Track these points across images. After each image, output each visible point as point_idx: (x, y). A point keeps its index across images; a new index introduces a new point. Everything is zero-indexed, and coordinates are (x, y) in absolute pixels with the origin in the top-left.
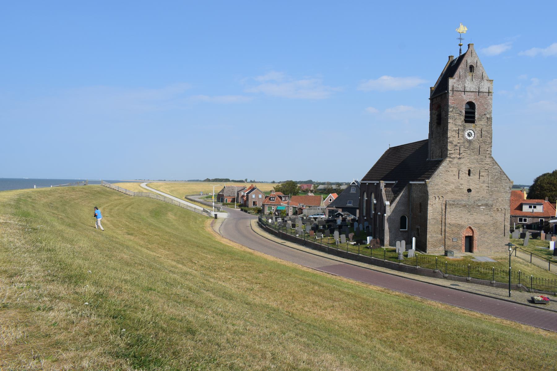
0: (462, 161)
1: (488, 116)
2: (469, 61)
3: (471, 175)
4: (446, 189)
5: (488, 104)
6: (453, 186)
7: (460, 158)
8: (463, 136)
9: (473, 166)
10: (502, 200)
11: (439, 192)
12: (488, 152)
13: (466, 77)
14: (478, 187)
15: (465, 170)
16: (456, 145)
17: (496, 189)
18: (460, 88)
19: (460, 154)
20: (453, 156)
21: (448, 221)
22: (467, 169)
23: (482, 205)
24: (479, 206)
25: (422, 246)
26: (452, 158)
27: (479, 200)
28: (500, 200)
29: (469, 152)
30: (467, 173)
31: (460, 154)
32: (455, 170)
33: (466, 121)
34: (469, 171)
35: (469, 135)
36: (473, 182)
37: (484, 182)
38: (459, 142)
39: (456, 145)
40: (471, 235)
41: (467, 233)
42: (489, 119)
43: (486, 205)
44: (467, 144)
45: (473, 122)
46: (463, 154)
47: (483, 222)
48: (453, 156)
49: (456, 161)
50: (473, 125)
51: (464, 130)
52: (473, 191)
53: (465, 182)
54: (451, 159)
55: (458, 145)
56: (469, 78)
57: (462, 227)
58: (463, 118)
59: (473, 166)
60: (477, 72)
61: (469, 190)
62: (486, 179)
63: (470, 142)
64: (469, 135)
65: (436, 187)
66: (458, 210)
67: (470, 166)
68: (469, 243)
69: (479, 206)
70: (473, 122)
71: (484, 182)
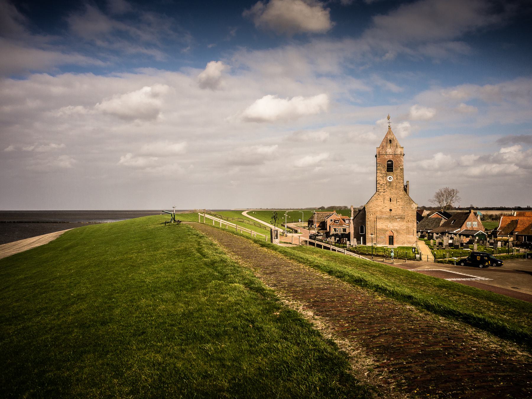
1: (401, 167)
5: (401, 161)
6: (381, 208)
8: (386, 179)
9: (392, 196)
13: (387, 146)
14: (396, 208)
15: (388, 198)
20: (380, 191)
21: (378, 227)
25: (365, 243)
27: (397, 215)
28: (410, 215)
32: (381, 199)
33: (388, 171)
36: (394, 205)
37: (400, 205)
41: (388, 234)
42: (402, 170)
44: (388, 184)
45: (392, 171)
48: (380, 191)
49: (382, 193)
51: (386, 176)
53: (388, 205)
56: (389, 147)
57: (387, 231)
59: (392, 196)
60: (394, 143)
61: (391, 210)
62: (401, 203)
63: (390, 183)
68: (391, 240)
70: (392, 171)
71: (400, 205)
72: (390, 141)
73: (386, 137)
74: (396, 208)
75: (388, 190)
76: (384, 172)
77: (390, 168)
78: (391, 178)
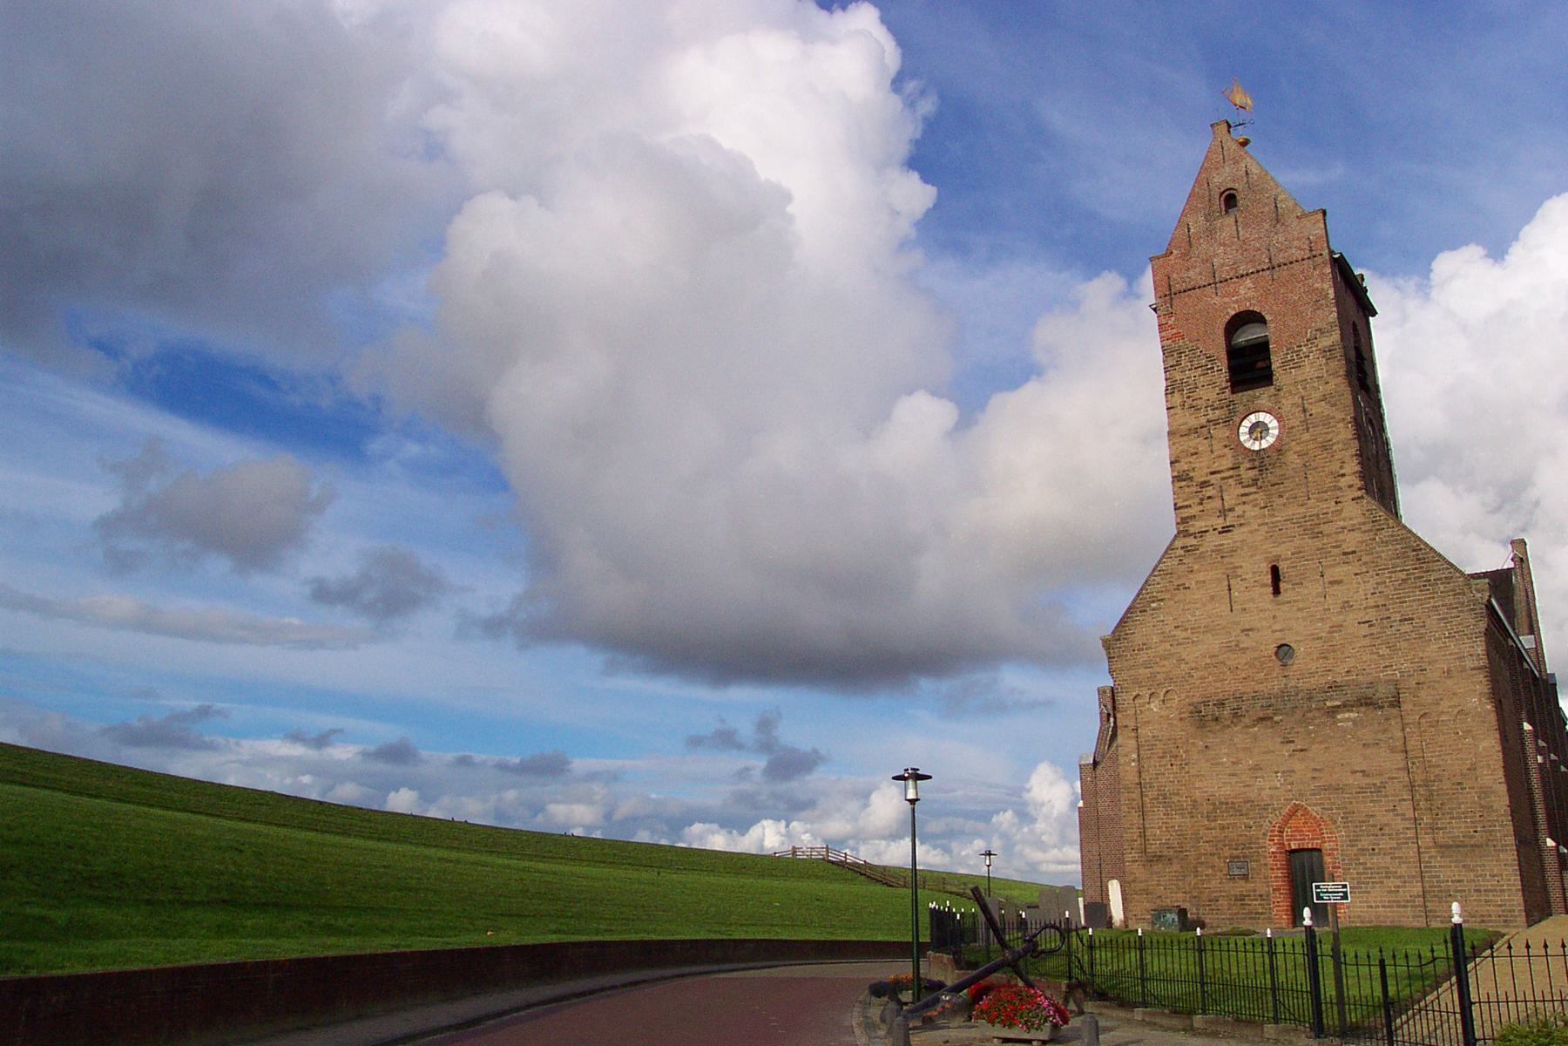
0: (1237, 534)
1: (1326, 342)
2: (1217, 180)
3: (1282, 585)
4: (1181, 660)
6: (1212, 643)
7: (1226, 530)
10: (1448, 673)
11: (1153, 677)
12: (1343, 482)
13: (1210, 233)
16: (1204, 484)
17: (1406, 627)
18: (1195, 275)
19: (1223, 512)
20: (1197, 525)
22: (1265, 568)
23: (1345, 706)
24: (1334, 711)
26: (1194, 535)
27: (1333, 687)
29: (1260, 497)
30: (1268, 579)
31: (1223, 512)
34: (1275, 571)
35: (1259, 429)
37: (1346, 605)
38: (1215, 467)
39: (1204, 484)
40: (1315, 844)
43: (1367, 702)
45: (1266, 378)
46: (1239, 510)
47: (1359, 780)
49: (1212, 540)
50: (1263, 395)
51: (1232, 420)
52: (1300, 650)
54: (1191, 541)
55: (1214, 479)
58: (1222, 375)
59: (1285, 550)
64: (1259, 429)
65: (1142, 657)
66: (1238, 735)
67: (1276, 551)
69: (1334, 711)
71: (1346, 605)
72: (1230, 200)
73: (1203, 180)
74: (1322, 628)
75: (1251, 512)
76: (1210, 395)
77: (1249, 367)
78: (1261, 428)
